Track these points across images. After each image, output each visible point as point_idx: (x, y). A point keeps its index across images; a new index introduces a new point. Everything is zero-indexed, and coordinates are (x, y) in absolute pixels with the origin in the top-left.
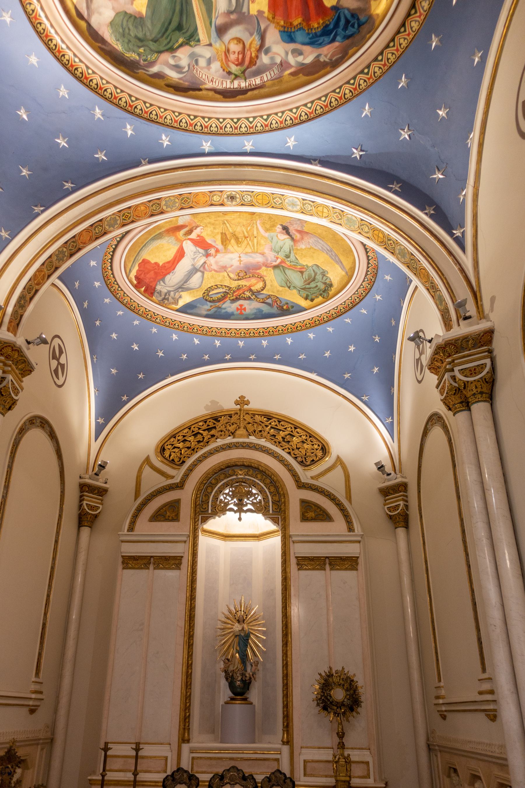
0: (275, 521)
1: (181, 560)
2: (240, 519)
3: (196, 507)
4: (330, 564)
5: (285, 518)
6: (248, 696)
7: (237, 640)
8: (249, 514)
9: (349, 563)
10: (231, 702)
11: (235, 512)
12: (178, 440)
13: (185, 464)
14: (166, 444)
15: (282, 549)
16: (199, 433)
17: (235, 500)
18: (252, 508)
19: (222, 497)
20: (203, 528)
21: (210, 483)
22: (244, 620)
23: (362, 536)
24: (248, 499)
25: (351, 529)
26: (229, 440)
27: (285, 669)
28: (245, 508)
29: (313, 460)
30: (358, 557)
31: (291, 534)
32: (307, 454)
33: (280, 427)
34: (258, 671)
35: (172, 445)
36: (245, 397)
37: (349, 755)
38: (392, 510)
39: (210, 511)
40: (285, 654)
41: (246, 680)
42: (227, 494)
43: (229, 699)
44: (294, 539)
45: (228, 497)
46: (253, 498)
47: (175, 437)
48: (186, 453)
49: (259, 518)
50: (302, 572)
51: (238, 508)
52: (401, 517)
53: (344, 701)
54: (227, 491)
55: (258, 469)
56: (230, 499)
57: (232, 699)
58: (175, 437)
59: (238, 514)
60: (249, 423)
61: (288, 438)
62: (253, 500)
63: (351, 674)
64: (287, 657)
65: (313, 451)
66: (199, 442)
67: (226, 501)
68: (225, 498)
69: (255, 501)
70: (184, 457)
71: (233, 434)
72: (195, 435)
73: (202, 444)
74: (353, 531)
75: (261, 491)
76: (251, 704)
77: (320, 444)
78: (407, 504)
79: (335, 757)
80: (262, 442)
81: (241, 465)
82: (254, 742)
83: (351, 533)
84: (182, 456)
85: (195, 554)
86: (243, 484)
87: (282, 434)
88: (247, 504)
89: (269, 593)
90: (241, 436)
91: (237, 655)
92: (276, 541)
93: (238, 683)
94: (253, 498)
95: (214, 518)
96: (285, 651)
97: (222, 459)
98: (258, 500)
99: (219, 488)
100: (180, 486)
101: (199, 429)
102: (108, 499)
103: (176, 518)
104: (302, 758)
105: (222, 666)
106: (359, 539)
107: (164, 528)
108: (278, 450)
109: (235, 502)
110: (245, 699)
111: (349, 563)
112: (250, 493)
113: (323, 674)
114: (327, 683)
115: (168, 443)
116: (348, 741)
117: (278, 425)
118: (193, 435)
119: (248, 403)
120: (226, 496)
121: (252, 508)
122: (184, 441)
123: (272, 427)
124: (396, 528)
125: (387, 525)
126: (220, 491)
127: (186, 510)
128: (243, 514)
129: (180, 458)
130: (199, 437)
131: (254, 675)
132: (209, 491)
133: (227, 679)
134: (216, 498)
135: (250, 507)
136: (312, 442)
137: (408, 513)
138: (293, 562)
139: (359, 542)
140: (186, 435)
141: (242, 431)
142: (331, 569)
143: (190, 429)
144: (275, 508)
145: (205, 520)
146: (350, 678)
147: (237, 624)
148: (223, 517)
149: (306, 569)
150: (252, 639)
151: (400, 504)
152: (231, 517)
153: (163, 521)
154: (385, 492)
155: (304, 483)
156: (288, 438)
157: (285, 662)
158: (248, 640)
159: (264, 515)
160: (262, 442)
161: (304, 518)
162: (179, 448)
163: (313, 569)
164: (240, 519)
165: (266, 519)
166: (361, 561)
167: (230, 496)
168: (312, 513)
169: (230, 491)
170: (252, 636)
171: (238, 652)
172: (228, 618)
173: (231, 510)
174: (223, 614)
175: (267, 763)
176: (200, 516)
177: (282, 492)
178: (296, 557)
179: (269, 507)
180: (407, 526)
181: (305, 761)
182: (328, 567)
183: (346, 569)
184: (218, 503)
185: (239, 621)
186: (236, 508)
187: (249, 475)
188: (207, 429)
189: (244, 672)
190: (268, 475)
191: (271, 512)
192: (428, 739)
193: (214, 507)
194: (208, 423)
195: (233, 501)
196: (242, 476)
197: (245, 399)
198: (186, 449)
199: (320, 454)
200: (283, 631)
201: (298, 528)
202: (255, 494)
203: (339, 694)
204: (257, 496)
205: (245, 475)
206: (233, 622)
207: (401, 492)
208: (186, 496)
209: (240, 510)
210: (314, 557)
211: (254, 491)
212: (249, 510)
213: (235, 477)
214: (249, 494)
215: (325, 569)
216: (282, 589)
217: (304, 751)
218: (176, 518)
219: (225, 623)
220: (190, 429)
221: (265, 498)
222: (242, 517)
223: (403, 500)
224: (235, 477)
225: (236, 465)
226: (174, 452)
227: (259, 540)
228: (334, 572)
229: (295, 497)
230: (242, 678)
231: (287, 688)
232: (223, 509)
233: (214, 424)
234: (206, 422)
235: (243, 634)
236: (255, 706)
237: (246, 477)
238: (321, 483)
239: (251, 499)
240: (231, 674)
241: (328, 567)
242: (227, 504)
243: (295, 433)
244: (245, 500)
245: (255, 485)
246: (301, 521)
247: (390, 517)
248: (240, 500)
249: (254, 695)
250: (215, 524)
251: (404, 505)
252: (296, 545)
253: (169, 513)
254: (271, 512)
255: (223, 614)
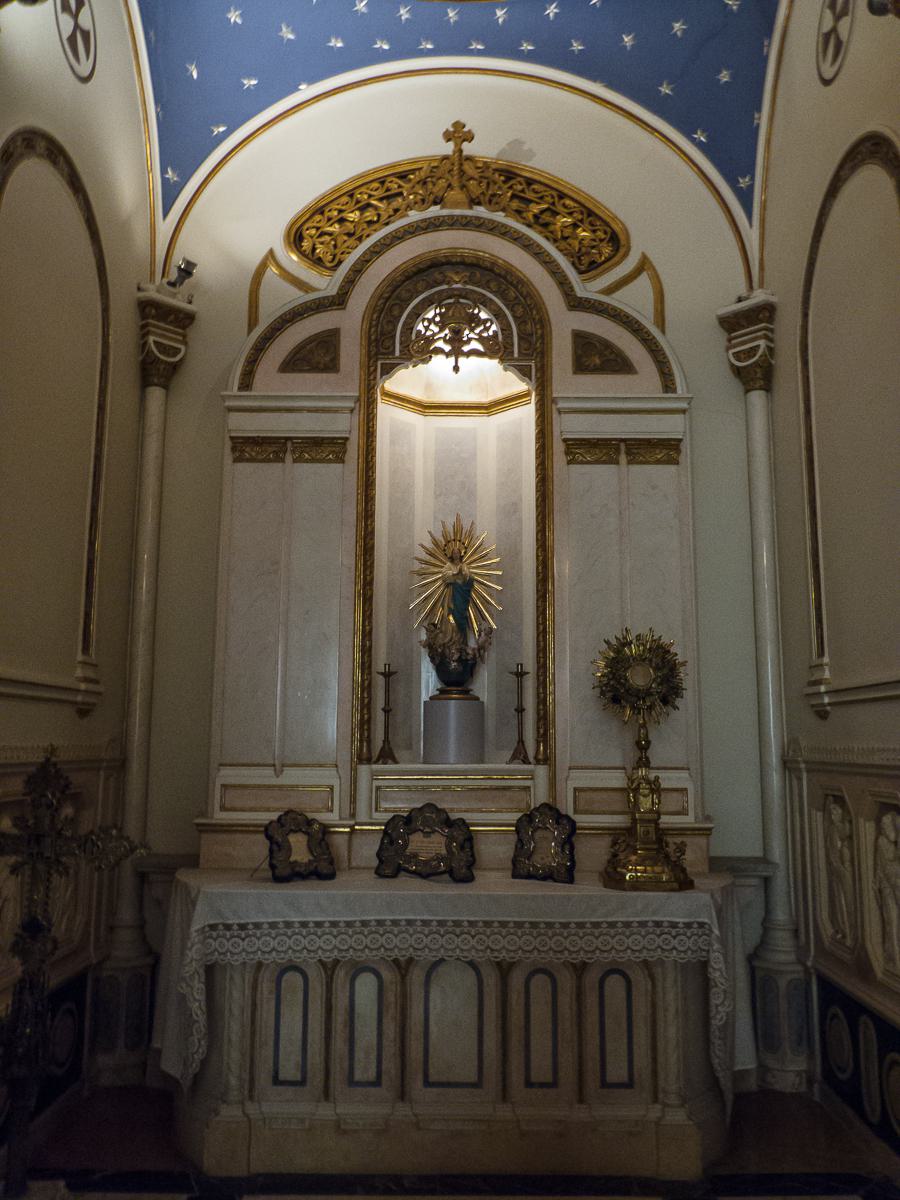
0: (524, 372)
1: (344, 444)
2: (456, 369)
3: (369, 344)
4: (628, 453)
5: (543, 366)
6: (471, 687)
7: (448, 592)
8: (473, 359)
9: (667, 450)
10: (442, 696)
11: (448, 355)
12: (329, 219)
13: (343, 264)
14: (305, 227)
15: (537, 425)
16: (369, 205)
17: (447, 331)
18: (480, 347)
19: (420, 327)
20: (383, 387)
21: (397, 298)
22: (462, 557)
23: (690, 400)
24: (472, 330)
25: (668, 385)
26: (435, 211)
27: (541, 638)
28: (466, 348)
29: (593, 262)
30: (680, 440)
31: (554, 395)
32: (584, 250)
33: (529, 195)
34: (490, 644)
35: (318, 229)
36: (464, 126)
37: (657, 778)
38: (743, 356)
39: (397, 353)
40: (541, 613)
41: (467, 660)
42: (431, 321)
43: (438, 692)
44: (561, 405)
45: (432, 327)
46: (482, 328)
47: (322, 213)
48: (346, 245)
49: (492, 365)
50: (574, 468)
51: (453, 348)
52: (758, 370)
53: (651, 687)
54: (430, 315)
55: (491, 270)
56: (436, 329)
57: (442, 691)
58: (322, 213)
59: (452, 360)
60: (472, 178)
61: (546, 217)
62: (481, 332)
63: (665, 640)
64: (545, 619)
65: (595, 244)
66: (370, 223)
67: (429, 333)
68: (427, 328)
69: (485, 335)
70: (342, 253)
71: (438, 201)
72: (362, 209)
73: (376, 226)
74: (674, 391)
75: (498, 315)
76: (477, 699)
77: (608, 230)
78: (772, 345)
79: (632, 783)
80: (500, 217)
81: (457, 263)
82: (483, 762)
83: (670, 395)
84: (337, 251)
85: (370, 434)
86: (462, 300)
87: (535, 209)
88: (470, 340)
89: (511, 510)
90: (456, 205)
91: (451, 618)
92: (527, 413)
93: (454, 664)
94: (482, 328)
95: (407, 367)
96: (541, 609)
97: (420, 251)
98: (491, 333)
99: (414, 308)
100: (340, 301)
101: (370, 196)
102: (192, 333)
103: (332, 366)
104: (571, 785)
105: (424, 636)
106: (684, 405)
107: (307, 385)
108: (534, 235)
109: (446, 335)
110: (467, 692)
111: (667, 450)
112: (474, 321)
113: (614, 642)
114: (618, 661)
115: (309, 224)
116: (658, 753)
117: (526, 190)
118: (359, 209)
119: (469, 137)
120: (428, 323)
121: (480, 347)
122: (342, 221)
123: (514, 196)
124: (747, 391)
125: (735, 385)
126: (417, 314)
127: (351, 351)
128: (462, 360)
129: (335, 256)
130: (370, 215)
131: (482, 651)
132: (396, 313)
133: (433, 660)
134: (409, 327)
135: (475, 345)
136: (593, 225)
137: (773, 362)
138: (558, 448)
139: (684, 411)
140: (343, 208)
141: (455, 194)
142: (630, 462)
143: (351, 196)
144: (523, 347)
145: (388, 370)
146: (663, 648)
147: (449, 564)
148: (420, 366)
149: (582, 463)
150: (476, 592)
151: (758, 346)
152: (440, 364)
153: (308, 371)
154: (731, 324)
155: (581, 298)
156: (546, 217)
157: (541, 627)
158: (469, 591)
159: (502, 360)
160: (500, 217)
161: (581, 367)
162: (330, 234)
163: (597, 462)
164: (456, 369)
165: (506, 369)
166: (685, 447)
167: (436, 324)
168: (594, 356)
169: (436, 315)
170: (476, 586)
171: (451, 612)
172: (431, 555)
173: (439, 351)
174: (422, 546)
175: (508, 793)
176: (379, 363)
177: (537, 317)
178: (565, 440)
179: (512, 345)
180: (768, 388)
181: (575, 789)
182: (623, 458)
183: (658, 462)
184: (413, 337)
185: (452, 559)
186: (447, 348)
187: (474, 284)
188: (387, 198)
189: (463, 646)
190: (511, 284)
191: (516, 355)
192: (783, 756)
193: (405, 345)
194: (387, 184)
195: (442, 335)
196: (459, 286)
197: (466, 129)
198: (345, 238)
199: (607, 250)
200: (538, 574)
201: (567, 384)
202: (486, 321)
203: (639, 678)
204: (488, 324)
205: (465, 283)
206: (441, 561)
207: (762, 322)
208: (351, 322)
209: (456, 352)
210: (598, 440)
211: (483, 315)
212: (474, 352)
213: (445, 287)
214: (473, 322)
215: (617, 463)
216: (537, 500)
217: (574, 773)
218: (332, 366)
219: (426, 563)
220: (351, 196)
221: (505, 328)
222: (459, 365)
223: (766, 337)
224: (445, 287)
225: (448, 263)
226: (322, 243)
227: (489, 414)
228: (636, 468)
229: (564, 324)
230: (460, 657)
231: (545, 672)
232: (423, 351)
233: (400, 187)
234: (383, 183)
235: (460, 582)
236: (483, 703)
237: (468, 287)
238: (615, 300)
239: (477, 331)
240: (440, 650)
241: (623, 458)
242: (430, 340)
243: (560, 208)
244: (467, 332)
245: (485, 303)
246: (575, 373)
247: (738, 372)
248: (457, 333)
249: (484, 685)
250: (405, 380)
251: (768, 347)
252: (565, 417)
253: (319, 355)
254: (516, 355)
255: (422, 546)
